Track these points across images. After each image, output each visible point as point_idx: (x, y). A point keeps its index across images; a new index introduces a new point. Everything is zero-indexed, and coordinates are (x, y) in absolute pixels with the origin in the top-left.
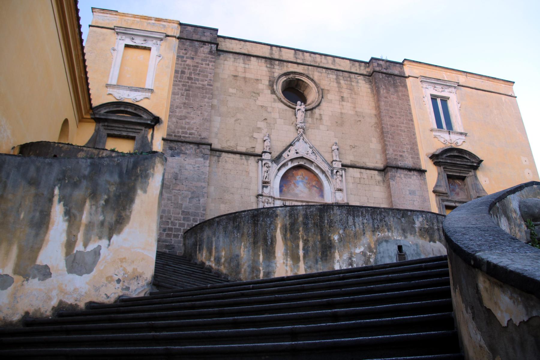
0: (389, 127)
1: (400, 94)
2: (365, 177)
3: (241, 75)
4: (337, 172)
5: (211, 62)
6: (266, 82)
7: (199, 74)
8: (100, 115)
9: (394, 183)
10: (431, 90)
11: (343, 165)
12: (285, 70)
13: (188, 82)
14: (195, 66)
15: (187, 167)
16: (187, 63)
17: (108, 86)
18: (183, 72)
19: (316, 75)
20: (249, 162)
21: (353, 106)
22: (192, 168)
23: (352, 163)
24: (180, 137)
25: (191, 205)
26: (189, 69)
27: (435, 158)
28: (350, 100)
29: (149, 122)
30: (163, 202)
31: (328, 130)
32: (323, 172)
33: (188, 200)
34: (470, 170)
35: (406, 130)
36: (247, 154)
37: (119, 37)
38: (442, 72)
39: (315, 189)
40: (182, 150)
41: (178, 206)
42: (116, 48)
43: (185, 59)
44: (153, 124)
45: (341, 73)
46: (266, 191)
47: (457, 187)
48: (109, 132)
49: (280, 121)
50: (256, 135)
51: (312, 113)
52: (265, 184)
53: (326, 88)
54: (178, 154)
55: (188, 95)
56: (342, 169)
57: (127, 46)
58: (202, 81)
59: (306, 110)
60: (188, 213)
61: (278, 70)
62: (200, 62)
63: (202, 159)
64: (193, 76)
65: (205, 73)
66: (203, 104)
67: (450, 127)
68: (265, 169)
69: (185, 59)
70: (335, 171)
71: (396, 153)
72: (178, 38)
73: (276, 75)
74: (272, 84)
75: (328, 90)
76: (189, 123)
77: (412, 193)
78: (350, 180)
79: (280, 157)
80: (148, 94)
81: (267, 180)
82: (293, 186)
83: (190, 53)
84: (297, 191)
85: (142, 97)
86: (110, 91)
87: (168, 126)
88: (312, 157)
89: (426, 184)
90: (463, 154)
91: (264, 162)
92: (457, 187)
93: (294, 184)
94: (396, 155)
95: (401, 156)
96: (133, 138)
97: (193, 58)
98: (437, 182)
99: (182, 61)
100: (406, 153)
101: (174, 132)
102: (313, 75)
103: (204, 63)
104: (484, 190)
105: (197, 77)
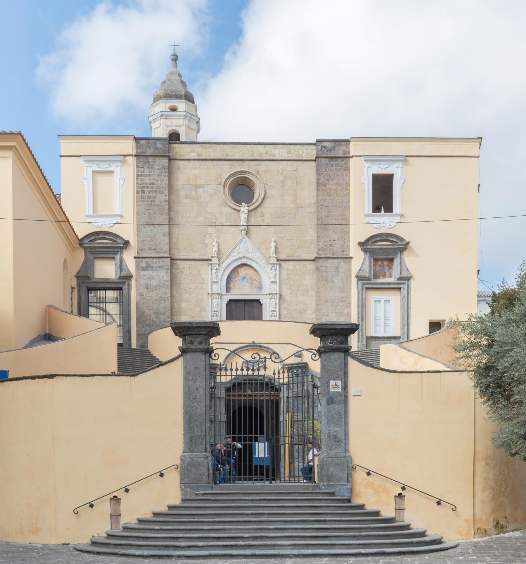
7: (156, 191)
11: (278, 260)
13: (148, 201)
14: (152, 184)
26: (148, 187)
29: (122, 245)
48: (95, 256)
57: (94, 172)
59: (249, 211)
62: (156, 178)
65: (161, 190)
72: (136, 156)
78: (284, 272)
80: (118, 220)
89: (349, 270)
103: (159, 178)
105: (154, 195)
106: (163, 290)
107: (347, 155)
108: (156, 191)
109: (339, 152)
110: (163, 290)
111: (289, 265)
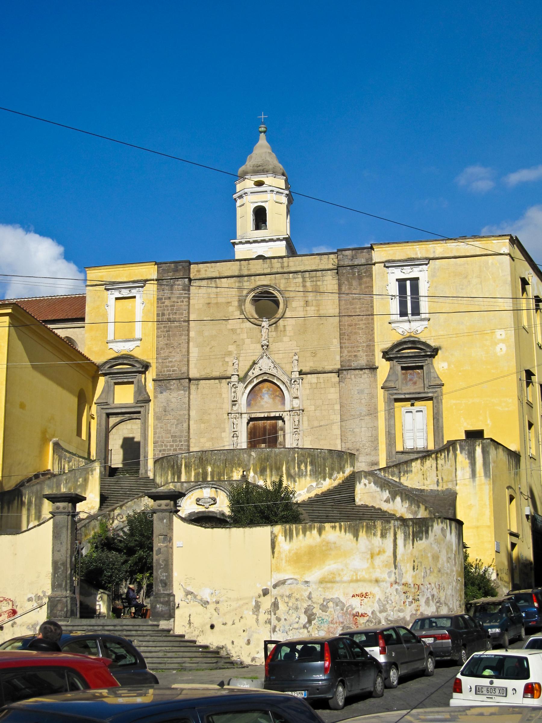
0: (346, 327)
1: (363, 286)
2: (322, 381)
3: (214, 301)
4: (294, 382)
5: (184, 298)
6: (236, 304)
8: (105, 370)
9: (344, 385)
10: (399, 274)
12: (252, 286)
16: (166, 304)
19: (281, 282)
20: (222, 385)
21: (317, 309)
22: (176, 401)
23: (312, 369)
25: (177, 430)
26: (168, 310)
27: (386, 355)
28: (314, 303)
30: (157, 431)
31: (291, 341)
33: (175, 427)
34: (426, 359)
35: (364, 327)
36: (220, 378)
37: (109, 292)
38: (415, 247)
39: (278, 398)
40: (167, 387)
41: (168, 431)
42: (109, 303)
43: (163, 300)
44: (143, 370)
46: (235, 408)
47: (415, 376)
49: (248, 341)
50: (227, 359)
51: (277, 326)
52: (234, 402)
53: (292, 294)
54: (165, 390)
55: (169, 336)
56: (299, 379)
57: (117, 299)
60: (175, 436)
62: (176, 300)
63: (182, 392)
64: (171, 317)
66: (180, 342)
67: (416, 311)
68: (233, 390)
69: (163, 300)
70: (293, 381)
71: (350, 354)
73: (245, 292)
74: (241, 302)
77: (361, 392)
79: (246, 374)
80: (138, 343)
81: (235, 399)
82: (259, 399)
83: (167, 293)
84: (262, 403)
85: (133, 347)
86: (110, 345)
87: (156, 368)
88: (274, 372)
89: (376, 381)
90: (416, 344)
91: (232, 384)
92: (415, 376)
93: (261, 397)
94: (350, 356)
95: (355, 356)
96: (132, 383)
97: (170, 298)
98: (388, 377)
99: (161, 303)
100: (361, 352)
101: (161, 372)
102: (280, 283)
103: (179, 300)
104: (438, 377)
106: (182, 412)
107: (370, 262)
108: (176, 313)
110: (182, 412)
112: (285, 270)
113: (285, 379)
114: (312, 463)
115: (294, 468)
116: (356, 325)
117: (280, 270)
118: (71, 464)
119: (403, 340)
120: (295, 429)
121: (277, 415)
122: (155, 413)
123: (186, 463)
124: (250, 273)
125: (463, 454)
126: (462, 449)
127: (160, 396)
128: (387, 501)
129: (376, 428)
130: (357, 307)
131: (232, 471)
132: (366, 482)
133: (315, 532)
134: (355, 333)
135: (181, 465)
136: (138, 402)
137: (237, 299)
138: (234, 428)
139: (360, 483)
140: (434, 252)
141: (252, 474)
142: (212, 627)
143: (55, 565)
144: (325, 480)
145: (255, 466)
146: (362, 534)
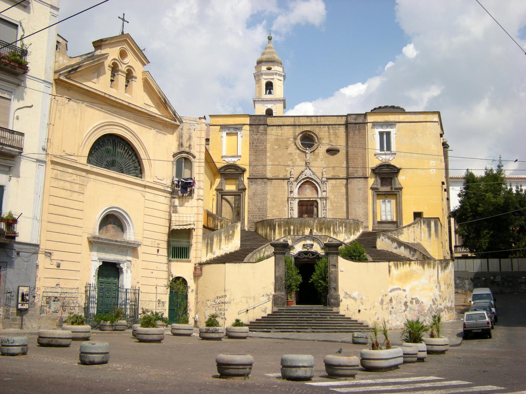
0: (352, 155)
1: (361, 134)
2: (338, 183)
6: (292, 140)
7: (260, 143)
8: (222, 172)
11: (327, 179)
13: (256, 148)
15: (258, 189)
17: (222, 157)
18: (253, 143)
19: (316, 130)
20: (284, 182)
24: (254, 175)
26: (255, 141)
30: (250, 205)
32: (317, 183)
41: (256, 206)
45: (331, 126)
46: (292, 195)
49: (298, 160)
50: (287, 169)
55: (256, 155)
58: (262, 146)
61: (299, 130)
64: (257, 145)
66: (263, 158)
67: (389, 148)
73: (297, 134)
74: (295, 139)
75: (323, 138)
76: (257, 169)
77: (359, 189)
81: (292, 190)
87: (249, 171)
88: (313, 177)
89: (367, 184)
93: (305, 189)
94: (354, 170)
95: (357, 171)
97: (257, 135)
99: (252, 137)
108: (260, 143)
109: (360, 120)
111: (333, 181)
112: (319, 123)
113: (319, 181)
114: (345, 227)
115: (337, 229)
116: (357, 154)
117: (316, 123)
118: (222, 223)
119: (382, 164)
120: (324, 207)
121: (314, 199)
122: (249, 196)
123: (278, 224)
124: (299, 124)
125: (425, 225)
126: (424, 223)
127: (251, 187)
128: (396, 248)
129: (367, 209)
130: (358, 145)
131: (304, 229)
132: (383, 238)
133: (407, 265)
134: (357, 159)
135: (276, 225)
136: (239, 190)
137: (292, 137)
138: (291, 205)
139: (379, 238)
140: (399, 118)
141: (315, 231)
142: (359, 311)
143: (276, 278)
144: (351, 235)
145: (317, 227)
146: (426, 266)
